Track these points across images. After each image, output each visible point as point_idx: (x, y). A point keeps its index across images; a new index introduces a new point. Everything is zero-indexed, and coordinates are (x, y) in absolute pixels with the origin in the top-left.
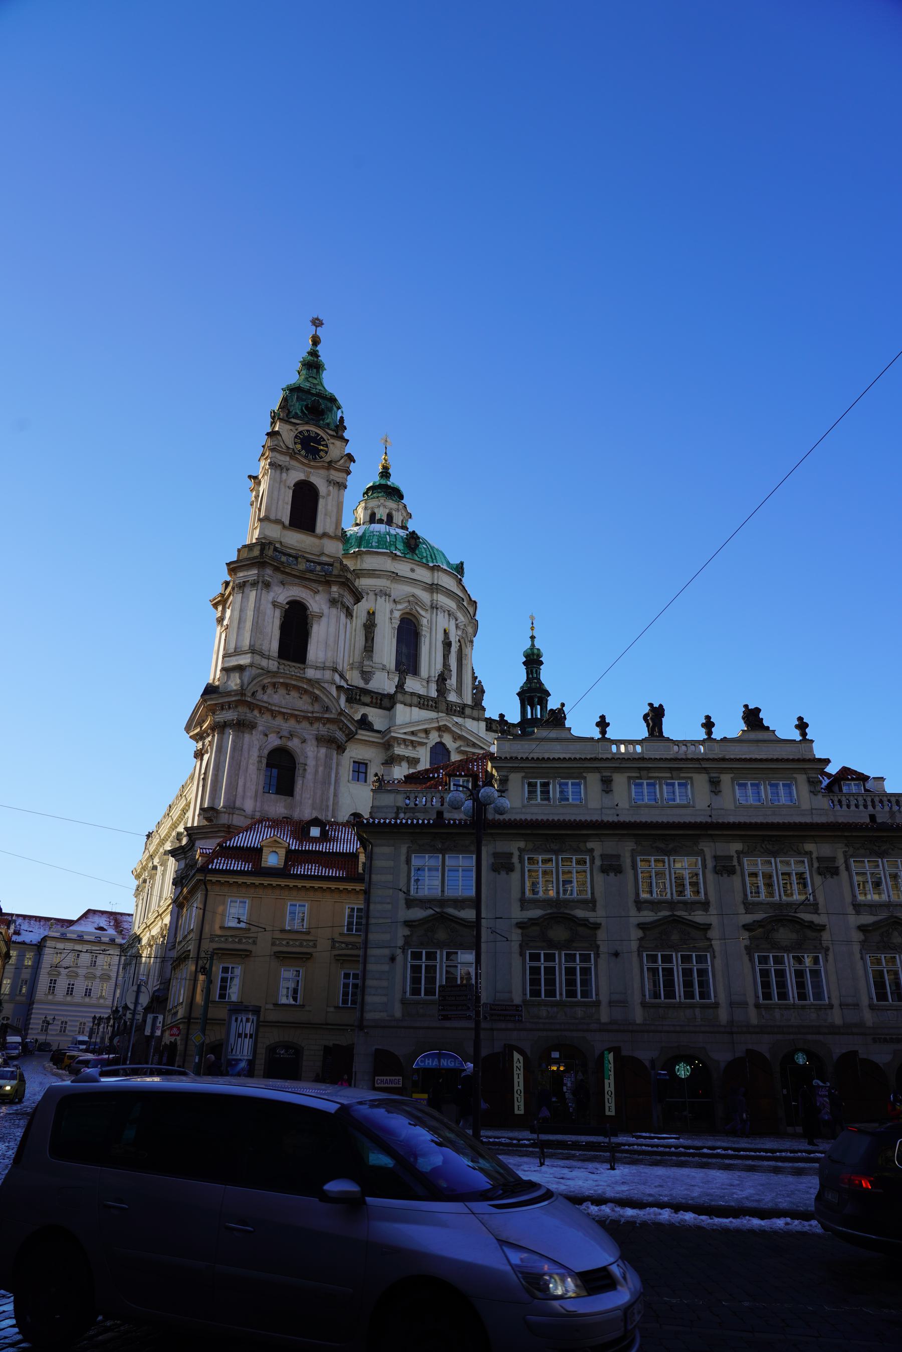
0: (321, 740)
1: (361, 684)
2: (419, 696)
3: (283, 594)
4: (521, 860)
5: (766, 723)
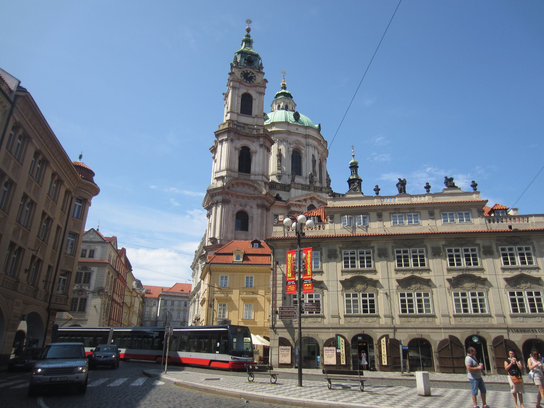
0: (258, 206)
2: (302, 185)
3: (240, 144)
4: (341, 253)
5: (456, 185)
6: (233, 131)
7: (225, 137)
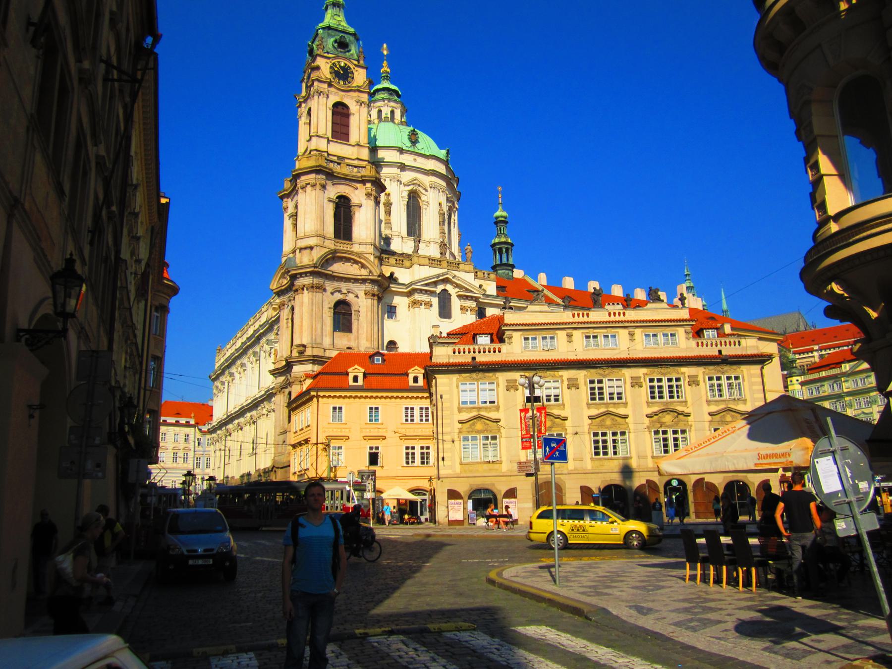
3: (334, 191)
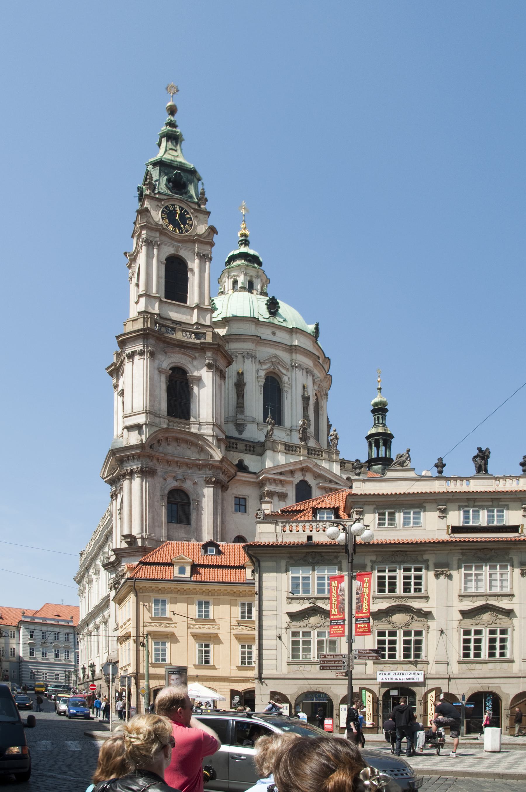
1: (236, 434)
6: (156, 336)
7: (139, 347)
